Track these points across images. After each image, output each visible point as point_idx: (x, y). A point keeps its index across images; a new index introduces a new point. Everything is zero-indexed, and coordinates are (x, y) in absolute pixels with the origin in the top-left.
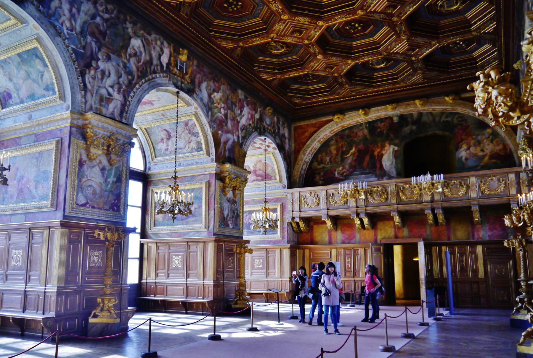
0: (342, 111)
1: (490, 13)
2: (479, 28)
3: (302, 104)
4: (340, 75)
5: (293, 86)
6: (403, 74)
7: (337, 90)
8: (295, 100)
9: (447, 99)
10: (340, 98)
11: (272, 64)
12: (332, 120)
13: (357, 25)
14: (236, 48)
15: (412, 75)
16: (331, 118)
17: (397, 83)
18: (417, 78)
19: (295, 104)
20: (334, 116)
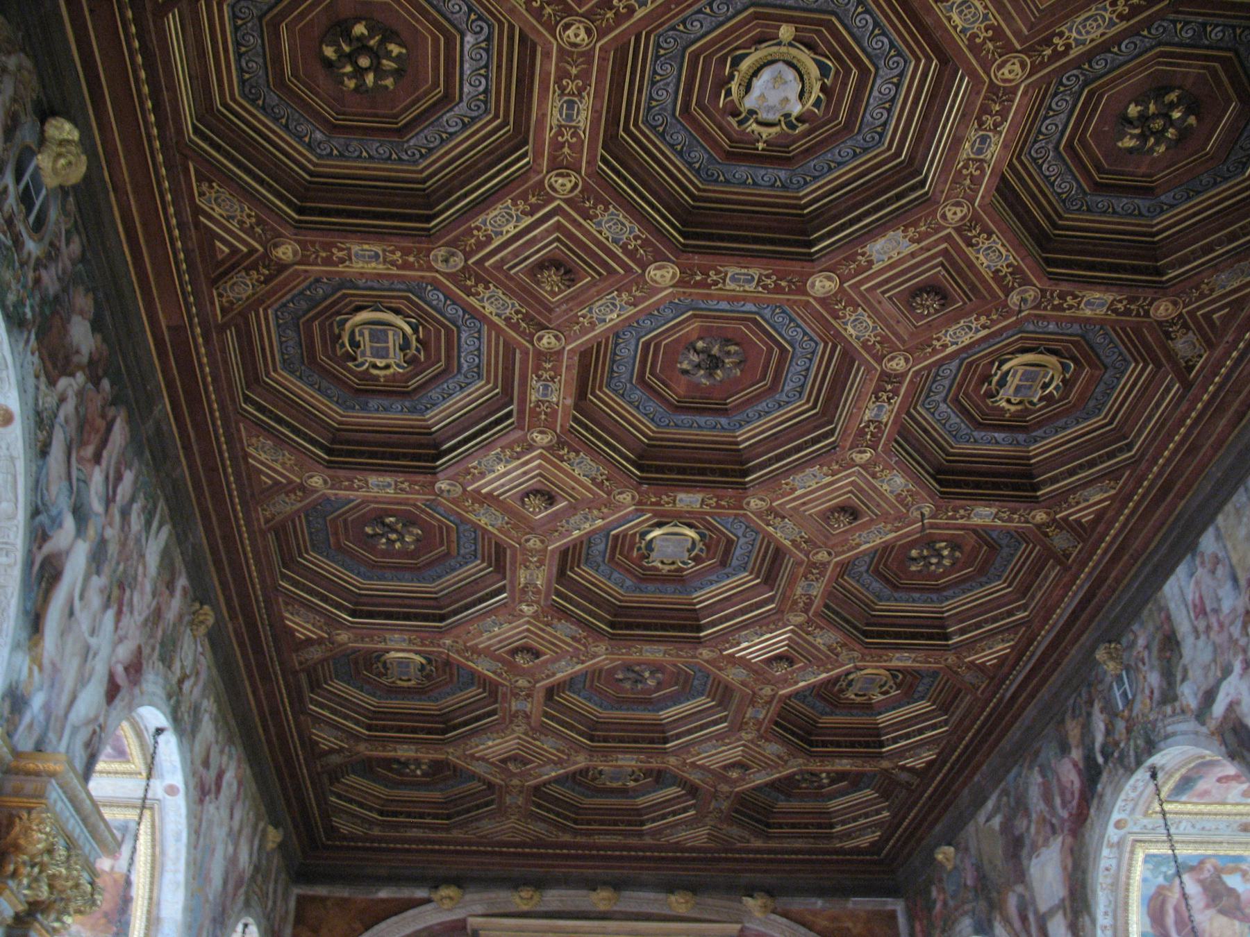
0: (459, 882)
1: (934, 727)
2: (901, 753)
3: (352, 837)
4: (523, 786)
5: (352, 779)
6: (664, 817)
7: (478, 819)
8: (339, 822)
9: (749, 901)
10: (470, 844)
11: (357, 708)
12: (428, 901)
13: (647, 674)
14: (320, 641)
15: (688, 823)
16: (421, 893)
17: (640, 834)
18: (697, 836)
19: (332, 830)
20: (436, 887)
